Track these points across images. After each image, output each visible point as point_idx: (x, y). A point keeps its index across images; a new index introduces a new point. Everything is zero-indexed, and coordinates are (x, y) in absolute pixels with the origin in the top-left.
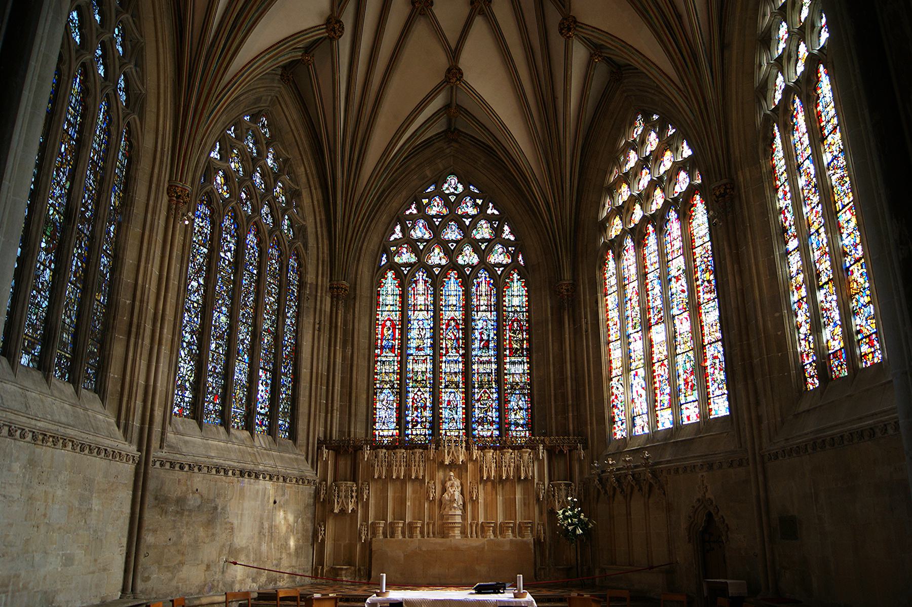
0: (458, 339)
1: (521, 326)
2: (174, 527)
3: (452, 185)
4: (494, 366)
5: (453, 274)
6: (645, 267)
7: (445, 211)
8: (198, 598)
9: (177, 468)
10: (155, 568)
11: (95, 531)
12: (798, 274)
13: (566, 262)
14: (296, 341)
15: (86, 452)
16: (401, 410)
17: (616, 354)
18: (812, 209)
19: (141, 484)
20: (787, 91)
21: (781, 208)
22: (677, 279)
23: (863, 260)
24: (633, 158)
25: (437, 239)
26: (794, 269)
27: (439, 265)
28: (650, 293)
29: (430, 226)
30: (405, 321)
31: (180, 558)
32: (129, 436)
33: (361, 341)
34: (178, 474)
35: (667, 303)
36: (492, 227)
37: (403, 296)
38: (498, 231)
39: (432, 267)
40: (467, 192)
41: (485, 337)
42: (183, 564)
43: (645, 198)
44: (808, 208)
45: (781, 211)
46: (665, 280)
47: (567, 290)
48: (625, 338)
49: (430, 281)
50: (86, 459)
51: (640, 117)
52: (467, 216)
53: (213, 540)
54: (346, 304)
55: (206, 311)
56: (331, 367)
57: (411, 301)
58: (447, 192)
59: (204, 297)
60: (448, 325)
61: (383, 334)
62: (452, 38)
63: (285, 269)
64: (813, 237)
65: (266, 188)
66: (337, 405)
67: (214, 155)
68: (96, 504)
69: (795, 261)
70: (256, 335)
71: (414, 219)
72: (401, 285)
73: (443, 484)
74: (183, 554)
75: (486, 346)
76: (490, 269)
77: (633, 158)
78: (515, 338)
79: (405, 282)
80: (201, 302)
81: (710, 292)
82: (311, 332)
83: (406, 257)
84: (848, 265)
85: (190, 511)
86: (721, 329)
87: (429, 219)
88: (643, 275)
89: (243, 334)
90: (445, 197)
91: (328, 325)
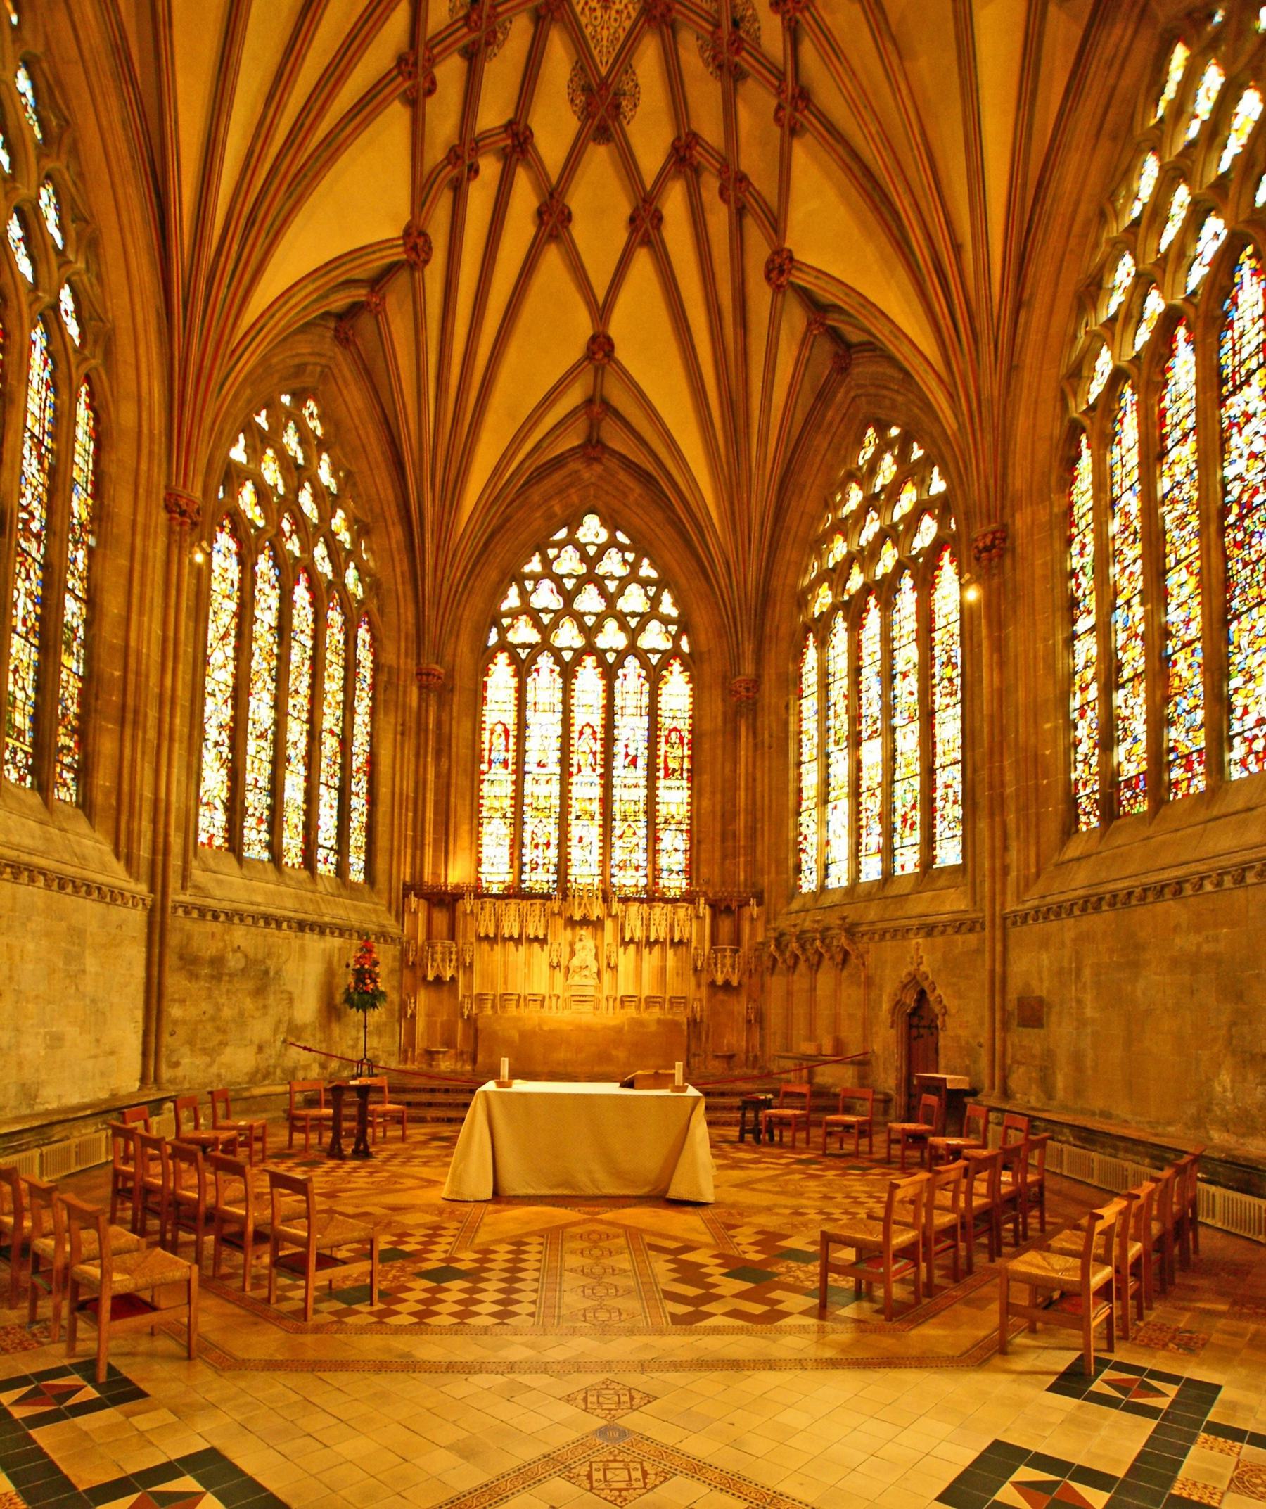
0: (594, 754)
1: (681, 738)
2: (210, 997)
3: (592, 530)
4: (645, 792)
5: (590, 661)
6: (860, 658)
7: (582, 569)
8: (247, 1089)
9: (209, 917)
10: (186, 1050)
11: (93, 1001)
12: (1085, 667)
13: (748, 648)
14: (371, 746)
15: (69, 889)
16: (517, 844)
17: (810, 778)
18: (1124, 569)
19: (157, 937)
20: (1118, 377)
21: (1073, 570)
22: (905, 675)
23: (1198, 645)
24: (855, 496)
25: (568, 610)
26: (1080, 661)
27: (570, 648)
28: (863, 695)
29: (561, 590)
30: (522, 725)
31: (220, 1037)
32: (134, 869)
33: (460, 749)
34: (210, 926)
35: (888, 709)
36: (646, 595)
37: (521, 691)
38: (655, 601)
39: (561, 650)
40: (613, 543)
41: (632, 752)
42: (226, 1044)
43: (869, 556)
44: (1118, 567)
45: (1073, 574)
46: (888, 677)
47: (747, 690)
48: (824, 757)
49: (557, 669)
50: (68, 901)
51: (871, 431)
52: (612, 578)
53: (265, 1014)
54: (440, 696)
55: (240, 694)
56: (420, 785)
57: (530, 697)
58: (583, 540)
59: (235, 676)
60: (581, 733)
61: (491, 744)
62: (600, 285)
63: (351, 644)
64: (1119, 612)
65: (321, 517)
66: (429, 838)
67: (238, 454)
68: (91, 964)
69: (1087, 648)
70: (314, 736)
71: (536, 578)
72: (517, 674)
73: (572, 945)
74: (224, 1032)
75: (634, 762)
76: (641, 655)
77: (855, 496)
78: (676, 755)
79: (523, 670)
80: (230, 682)
81: (951, 694)
82: (391, 736)
83: (524, 633)
84: (1170, 651)
85: (231, 975)
86: (963, 747)
87: (558, 579)
88: (855, 671)
89: (296, 731)
90: (581, 548)
91: (413, 725)
